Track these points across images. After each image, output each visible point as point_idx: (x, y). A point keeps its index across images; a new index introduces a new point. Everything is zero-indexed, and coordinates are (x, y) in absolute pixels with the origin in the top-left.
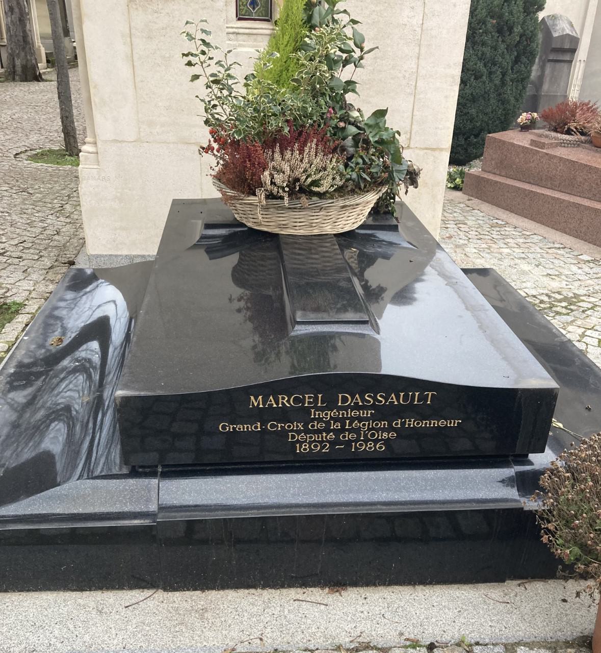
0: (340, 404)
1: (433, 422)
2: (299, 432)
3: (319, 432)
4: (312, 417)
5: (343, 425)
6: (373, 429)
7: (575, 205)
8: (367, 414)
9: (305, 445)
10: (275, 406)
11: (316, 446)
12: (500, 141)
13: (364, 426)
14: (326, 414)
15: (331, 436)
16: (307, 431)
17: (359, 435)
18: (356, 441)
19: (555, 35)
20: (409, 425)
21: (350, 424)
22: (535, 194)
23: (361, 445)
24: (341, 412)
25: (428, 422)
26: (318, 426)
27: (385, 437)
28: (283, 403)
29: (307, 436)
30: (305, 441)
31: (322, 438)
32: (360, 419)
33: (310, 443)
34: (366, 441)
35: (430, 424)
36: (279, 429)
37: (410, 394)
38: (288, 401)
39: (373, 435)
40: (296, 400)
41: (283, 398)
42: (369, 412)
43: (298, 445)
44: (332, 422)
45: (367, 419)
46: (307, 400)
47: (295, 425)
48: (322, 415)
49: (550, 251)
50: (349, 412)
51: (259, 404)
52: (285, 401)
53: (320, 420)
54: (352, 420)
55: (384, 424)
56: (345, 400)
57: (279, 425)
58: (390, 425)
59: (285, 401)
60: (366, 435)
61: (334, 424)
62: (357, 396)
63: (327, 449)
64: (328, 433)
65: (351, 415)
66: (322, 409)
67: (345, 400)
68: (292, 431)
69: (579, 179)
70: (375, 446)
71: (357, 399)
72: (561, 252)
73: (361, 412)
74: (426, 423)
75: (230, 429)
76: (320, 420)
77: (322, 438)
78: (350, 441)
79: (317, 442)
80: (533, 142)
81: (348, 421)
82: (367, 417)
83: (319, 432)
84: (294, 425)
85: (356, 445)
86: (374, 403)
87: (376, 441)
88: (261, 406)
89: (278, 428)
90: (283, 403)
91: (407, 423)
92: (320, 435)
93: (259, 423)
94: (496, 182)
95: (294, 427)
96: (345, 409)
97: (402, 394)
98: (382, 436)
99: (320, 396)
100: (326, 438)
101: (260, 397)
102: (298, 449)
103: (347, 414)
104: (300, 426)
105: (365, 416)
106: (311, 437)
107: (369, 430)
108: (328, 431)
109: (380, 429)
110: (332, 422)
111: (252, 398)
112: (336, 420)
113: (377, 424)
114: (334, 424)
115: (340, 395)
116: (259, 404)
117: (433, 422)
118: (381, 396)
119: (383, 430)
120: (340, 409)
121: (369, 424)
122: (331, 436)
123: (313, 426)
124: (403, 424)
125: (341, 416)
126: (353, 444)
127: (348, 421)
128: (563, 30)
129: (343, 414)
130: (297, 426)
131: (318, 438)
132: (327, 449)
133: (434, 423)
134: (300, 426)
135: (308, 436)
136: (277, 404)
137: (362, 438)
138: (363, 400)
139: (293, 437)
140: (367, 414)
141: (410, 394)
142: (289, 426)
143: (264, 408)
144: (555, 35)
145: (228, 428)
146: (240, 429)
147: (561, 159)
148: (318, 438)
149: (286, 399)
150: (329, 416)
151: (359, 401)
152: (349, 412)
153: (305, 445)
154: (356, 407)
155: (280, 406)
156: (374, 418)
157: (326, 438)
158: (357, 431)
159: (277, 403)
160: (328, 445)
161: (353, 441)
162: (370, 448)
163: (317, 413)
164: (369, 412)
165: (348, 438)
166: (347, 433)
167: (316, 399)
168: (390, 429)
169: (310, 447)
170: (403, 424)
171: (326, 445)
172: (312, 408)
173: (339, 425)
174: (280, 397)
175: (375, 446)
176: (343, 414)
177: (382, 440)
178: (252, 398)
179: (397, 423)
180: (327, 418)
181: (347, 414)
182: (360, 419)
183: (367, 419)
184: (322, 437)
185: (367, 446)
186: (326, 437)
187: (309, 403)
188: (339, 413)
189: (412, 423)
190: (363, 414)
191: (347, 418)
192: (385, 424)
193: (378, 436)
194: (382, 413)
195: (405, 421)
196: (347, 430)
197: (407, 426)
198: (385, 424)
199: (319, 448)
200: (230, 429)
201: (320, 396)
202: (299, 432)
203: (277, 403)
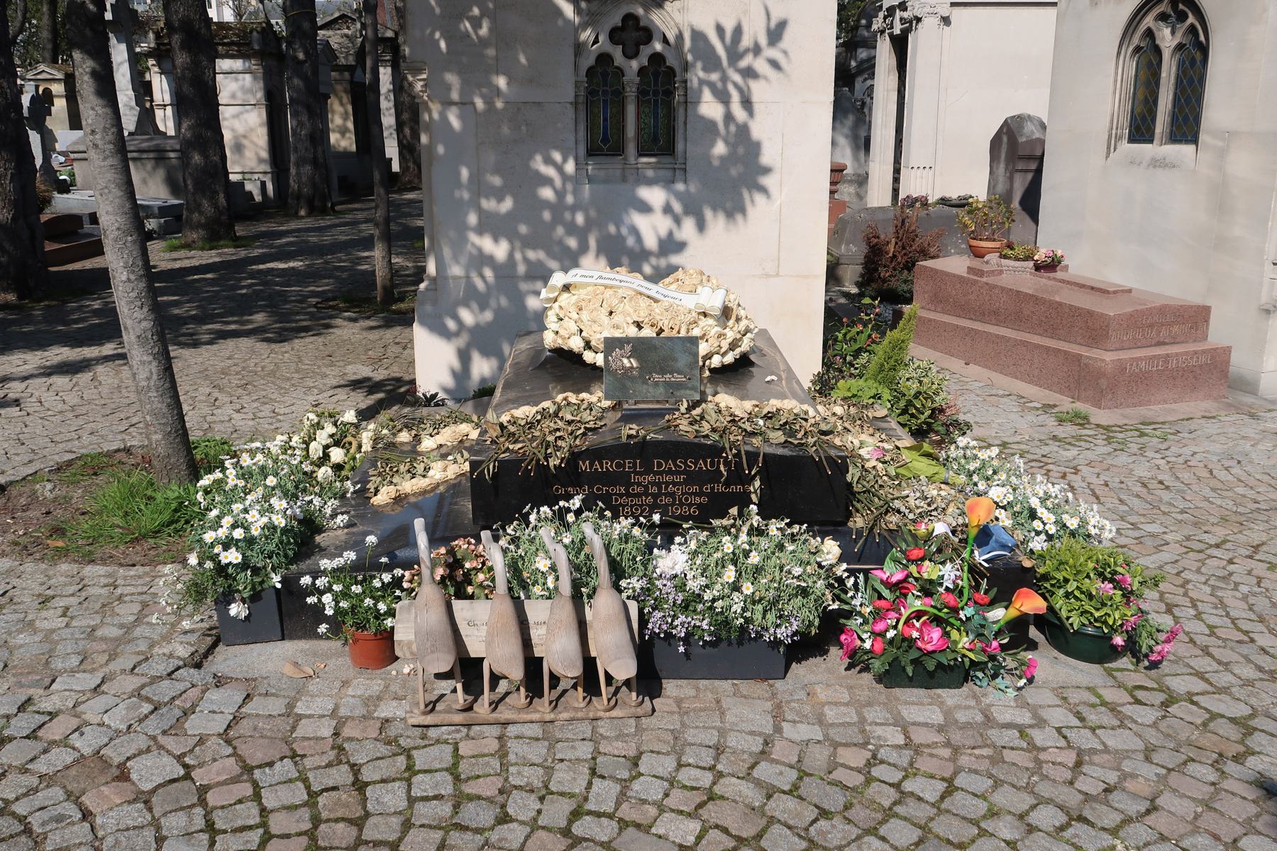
2: (621, 495)
3: (638, 495)
5: (660, 489)
7: (1025, 344)
12: (932, 269)
16: (628, 495)
17: (674, 499)
18: (672, 505)
19: (1022, 140)
21: (666, 488)
22: (977, 332)
26: (638, 490)
32: (675, 484)
33: (632, 506)
34: (681, 504)
39: (687, 499)
40: (618, 465)
45: (679, 484)
49: (988, 399)
52: (609, 465)
53: (639, 484)
54: (667, 484)
55: (695, 488)
56: (660, 465)
58: (701, 489)
59: (609, 465)
60: (680, 500)
66: (641, 474)
67: (660, 465)
69: (1026, 312)
72: (1005, 400)
76: (639, 484)
80: (971, 270)
83: (638, 495)
87: (690, 505)
94: (930, 320)
96: (661, 473)
107: (683, 494)
108: (646, 494)
112: (654, 484)
119: (696, 494)
120: (656, 473)
128: (1033, 132)
138: (676, 465)
144: (1022, 140)
147: (1003, 289)
154: (670, 472)
156: (686, 482)
158: (672, 495)
167: (635, 464)
168: (700, 494)
179: (707, 488)
182: (675, 484)
183: (679, 484)
194: (692, 478)
202: (621, 495)
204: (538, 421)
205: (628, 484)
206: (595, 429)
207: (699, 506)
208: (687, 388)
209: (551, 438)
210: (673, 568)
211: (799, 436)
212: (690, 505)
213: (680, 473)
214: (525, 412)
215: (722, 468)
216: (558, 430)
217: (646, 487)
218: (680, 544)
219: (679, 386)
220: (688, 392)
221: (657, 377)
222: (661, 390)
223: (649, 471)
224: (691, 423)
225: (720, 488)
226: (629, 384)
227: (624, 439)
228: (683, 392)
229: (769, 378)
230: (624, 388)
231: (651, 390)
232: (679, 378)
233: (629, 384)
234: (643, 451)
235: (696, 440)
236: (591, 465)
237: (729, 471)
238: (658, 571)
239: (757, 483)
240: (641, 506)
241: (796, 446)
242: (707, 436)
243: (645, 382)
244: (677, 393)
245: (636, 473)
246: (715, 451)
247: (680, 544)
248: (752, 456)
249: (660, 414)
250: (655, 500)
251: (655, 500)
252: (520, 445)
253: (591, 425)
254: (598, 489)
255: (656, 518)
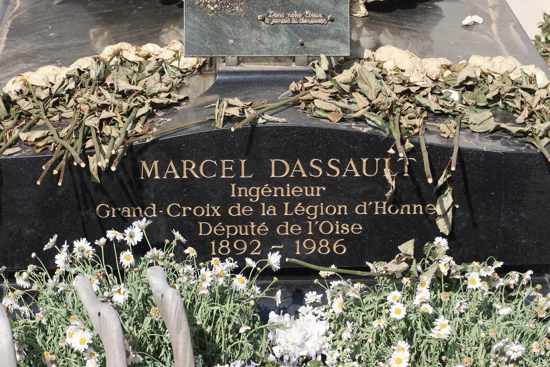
0: (273, 176)
1: (415, 206)
2: (214, 221)
3: (244, 221)
4: (233, 195)
5: (281, 209)
6: (326, 217)
8: (315, 193)
9: (225, 244)
10: (177, 177)
11: (240, 245)
13: (313, 212)
14: (254, 192)
15: (263, 228)
16: (225, 219)
17: (305, 227)
18: (302, 237)
20: (380, 210)
21: (291, 209)
23: (309, 244)
24: (276, 189)
25: (409, 207)
26: (242, 211)
27: (345, 231)
28: (189, 173)
29: (226, 229)
30: (224, 237)
31: (250, 231)
32: (306, 201)
34: (317, 236)
35: (412, 210)
36: (185, 215)
37: (377, 160)
38: (197, 170)
39: (326, 228)
40: (209, 169)
41: (189, 165)
42: (318, 189)
43: (213, 243)
44: (263, 204)
46: (224, 168)
47: (208, 208)
48: (248, 193)
50: (288, 189)
51: (153, 174)
52: (193, 169)
53: (245, 201)
54: (293, 201)
55: (341, 209)
56: (280, 169)
57: (184, 209)
58: (351, 209)
59: (193, 169)
60: (315, 228)
61: (266, 209)
62: (298, 162)
63: (257, 251)
64: (258, 224)
65: (291, 194)
66: (247, 183)
67: (280, 169)
68: (204, 218)
70: (331, 246)
71: (298, 168)
73: (306, 188)
74: (406, 209)
75: (111, 213)
76: (245, 201)
77: (250, 231)
78: (292, 237)
79: (244, 237)
81: (287, 204)
82: (315, 197)
83: (244, 221)
84: (206, 209)
85: (301, 244)
86: (324, 174)
88: (157, 177)
89: (182, 213)
90: (189, 173)
91: (377, 207)
92: (246, 227)
93: (154, 205)
95: (206, 213)
96: (282, 183)
97: (365, 161)
98: (340, 229)
99: (243, 162)
100: (255, 231)
101: (155, 163)
102: (213, 250)
103: (285, 193)
104: (216, 211)
105: (313, 195)
106: (232, 230)
107: (320, 218)
108: (257, 218)
109: (336, 217)
110: (263, 204)
111: (144, 164)
112: (270, 200)
113: (331, 210)
114: (266, 209)
115: (273, 162)
116: (153, 174)
117: (415, 206)
118: (333, 163)
119: (342, 219)
121: (319, 209)
122: (263, 228)
123: (234, 211)
124: (371, 209)
125: (276, 195)
126: (298, 242)
127: (287, 204)
129: (279, 192)
130: (211, 211)
131: (244, 231)
132: (257, 251)
133: (418, 209)
134: (216, 211)
135: (228, 227)
136: (181, 174)
137: (310, 233)
138: (308, 169)
139: (206, 229)
140: (315, 193)
141: (377, 160)
142: (199, 211)
143: (161, 180)
145: (108, 212)
146: (126, 213)
148: (244, 231)
149: (194, 166)
150: (258, 195)
151: (302, 170)
152: (288, 189)
153: (225, 244)
154: (297, 180)
155: (185, 177)
156: (325, 198)
157: (255, 231)
158: (302, 220)
159: (180, 173)
160: (259, 244)
161: (297, 238)
162: (324, 250)
163: (240, 189)
164: (318, 189)
165: (289, 232)
166: (287, 223)
168: (350, 219)
169: (231, 246)
170: (371, 209)
171: (257, 244)
172: (233, 181)
173: (274, 210)
174: (185, 162)
175: (331, 246)
176: (279, 192)
177: (341, 236)
178: (144, 164)
179: (362, 209)
180: (254, 198)
181: (285, 193)
182: (306, 201)
184: (250, 229)
185: (318, 246)
186: (255, 229)
187: (228, 173)
188: (273, 190)
189: (384, 207)
190: (309, 192)
191: (286, 199)
192: (343, 209)
193: (335, 230)
194: (335, 190)
195: (374, 205)
196: (288, 218)
197: (377, 213)
198: (343, 209)
199: (245, 248)
200: (111, 213)
201: (243, 162)
202: (214, 221)
203: (180, 173)
204: (71, 92)
205: (226, 201)
206: (169, 106)
207: (348, 239)
208: (328, 36)
209: (92, 122)
210: (302, 346)
211: (520, 119)
212: (333, 238)
213: (315, 182)
214: (48, 76)
215: (388, 174)
216: (105, 107)
217: (257, 206)
218: (314, 305)
219: (315, 32)
220: (329, 43)
221: (276, 16)
222: (283, 39)
223: (261, 178)
224: (334, 97)
225: (384, 208)
226: (227, 28)
227: (219, 124)
228: (320, 42)
229: (468, 20)
230: (218, 35)
231: (266, 38)
232: (316, 19)
233: (227, 28)
234: (251, 143)
235: (343, 126)
236: (162, 169)
237: (399, 178)
238: (276, 350)
239: (448, 200)
240: (248, 238)
241: (515, 136)
242: (362, 119)
243: (255, 25)
244: (311, 45)
245: (240, 182)
246: (375, 146)
247: (314, 305)
248: (439, 154)
249: (279, 80)
250: (272, 228)
251: (272, 228)
252: (39, 134)
253: (162, 99)
254: (174, 210)
255: (274, 260)
